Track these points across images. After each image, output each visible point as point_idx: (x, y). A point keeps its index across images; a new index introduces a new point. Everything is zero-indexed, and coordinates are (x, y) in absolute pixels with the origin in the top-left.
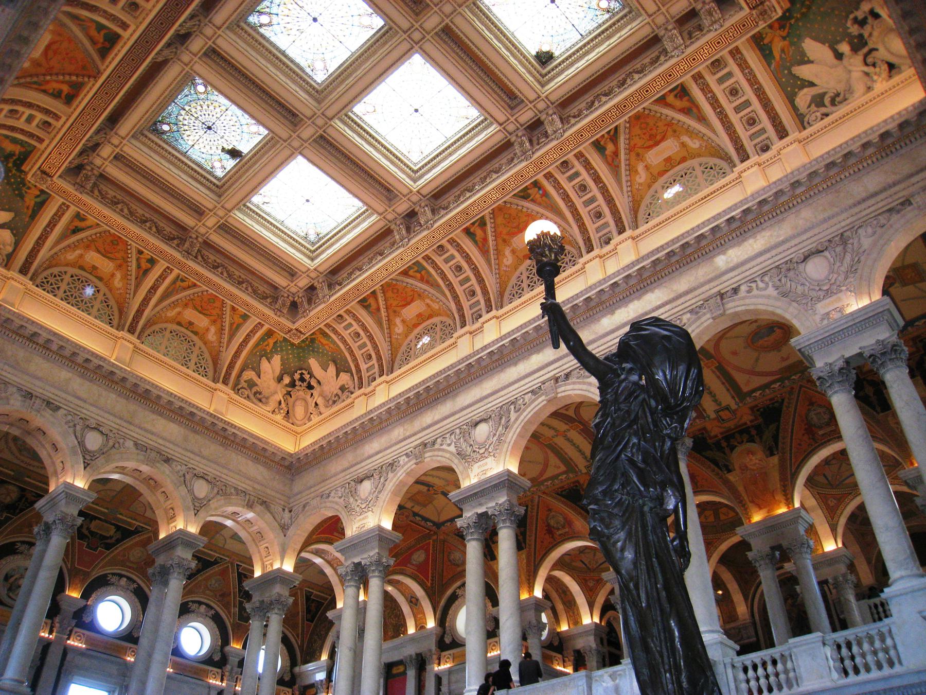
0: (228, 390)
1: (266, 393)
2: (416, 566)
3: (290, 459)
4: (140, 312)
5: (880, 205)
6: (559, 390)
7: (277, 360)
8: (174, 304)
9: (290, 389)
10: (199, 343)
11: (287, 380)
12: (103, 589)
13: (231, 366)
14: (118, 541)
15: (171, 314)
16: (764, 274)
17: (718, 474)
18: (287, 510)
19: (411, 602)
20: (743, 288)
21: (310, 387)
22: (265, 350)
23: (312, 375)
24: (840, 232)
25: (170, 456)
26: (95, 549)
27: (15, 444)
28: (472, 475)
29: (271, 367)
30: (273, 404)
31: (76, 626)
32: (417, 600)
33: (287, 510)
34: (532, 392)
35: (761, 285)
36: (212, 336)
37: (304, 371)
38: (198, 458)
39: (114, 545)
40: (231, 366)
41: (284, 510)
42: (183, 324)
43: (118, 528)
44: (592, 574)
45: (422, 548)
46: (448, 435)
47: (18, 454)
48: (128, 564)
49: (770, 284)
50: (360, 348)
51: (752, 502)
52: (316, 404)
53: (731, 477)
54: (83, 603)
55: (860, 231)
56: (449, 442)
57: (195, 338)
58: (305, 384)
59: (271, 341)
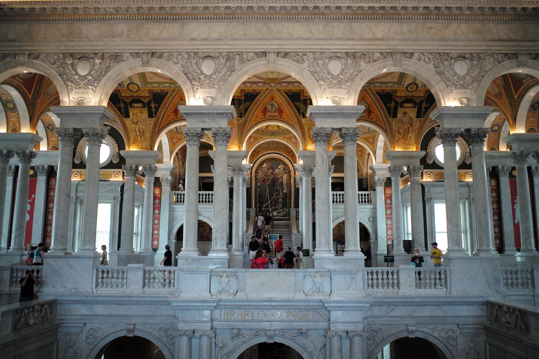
5: (503, 48)
6: (278, 63)
16: (431, 53)
17: (297, 116)
19: (48, 128)
20: (416, 55)
24: (479, 52)
28: (197, 96)
34: (256, 53)
35: (427, 60)
44: (177, 135)
46: (175, 54)
49: (432, 62)
51: (310, 138)
53: (303, 120)
55: (488, 57)
56: (175, 60)
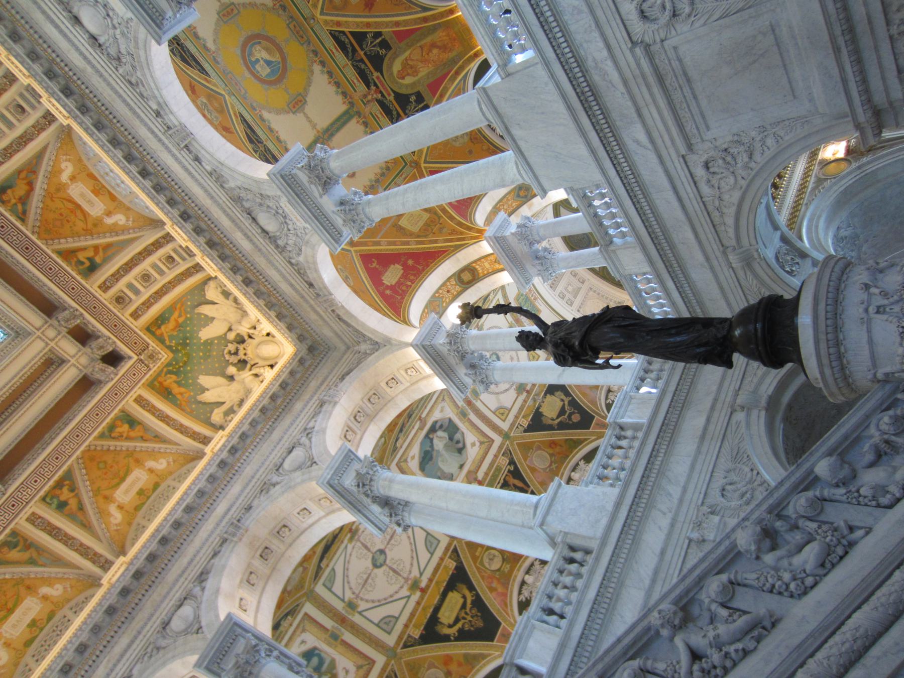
3: (304, 352)
8: (103, 514)
9: (249, 366)
11: (232, 370)
15: (117, 517)
18: (356, 348)
19: (526, 197)
33: (356, 348)
37: (226, 351)
42: (139, 502)
43: (451, 586)
50: (161, 273)
59: (176, 390)
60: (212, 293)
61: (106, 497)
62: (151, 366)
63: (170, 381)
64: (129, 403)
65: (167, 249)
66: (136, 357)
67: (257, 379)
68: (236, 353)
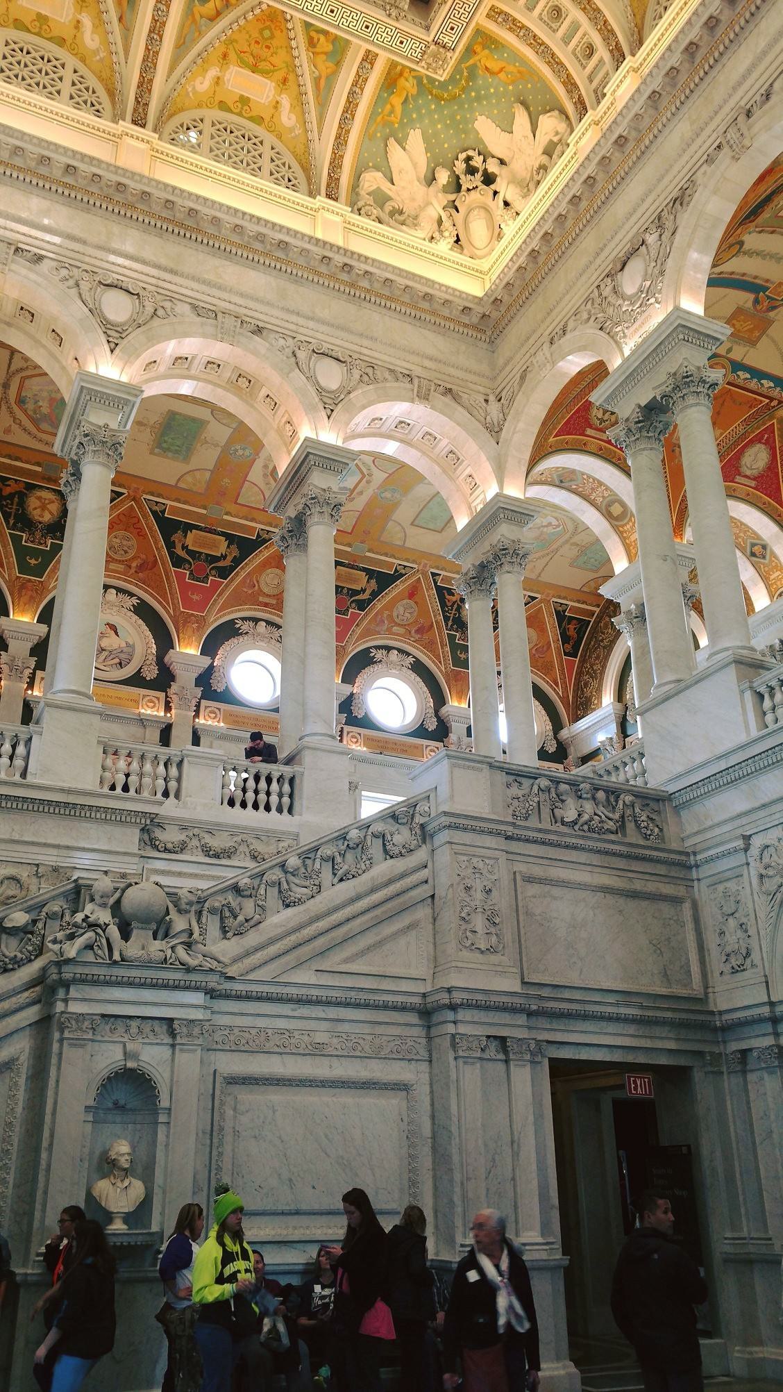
0: (342, 207)
1: (409, 209)
2: (755, 479)
3: (481, 310)
4: (145, 85)
7: (415, 139)
9: (452, 197)
10: (269, 139)
11: (443, 177)
12: (234, 641)
13: (336, 164)
14: (237, 562)
15: (203, 84)
18: (492, 398)
19: (753, 554)
21: (489, 179)
22: (387, 124)
23: (486, 156)
25: (261, 324)
26: (205, 580)
27: (25, 412)
29: (409, 158)
30: (428, 227)
31: (205, 696)
32: (764, 547)
33: (492, 398)
36: (287, 118)
37: (470, 153)
38: (311, 324)
39: (232, 569)
40: (336, 164)
41: (486, 401)
45: (758, 439)
47: (34, 430)
48: (261, 599)
50: (566, 41)
52: (506, 204)
54: (207, 661)
57: (259, 131)
58: (479, 176)
59: (397, 101)
60: (549, 124)
61: (225, 56)
62: (423, 64)
63: (408, 85)
64: (359, 48)
65: (602, 52)
66: (430, 39)
67: (436, 225)
68: (471, 171)
